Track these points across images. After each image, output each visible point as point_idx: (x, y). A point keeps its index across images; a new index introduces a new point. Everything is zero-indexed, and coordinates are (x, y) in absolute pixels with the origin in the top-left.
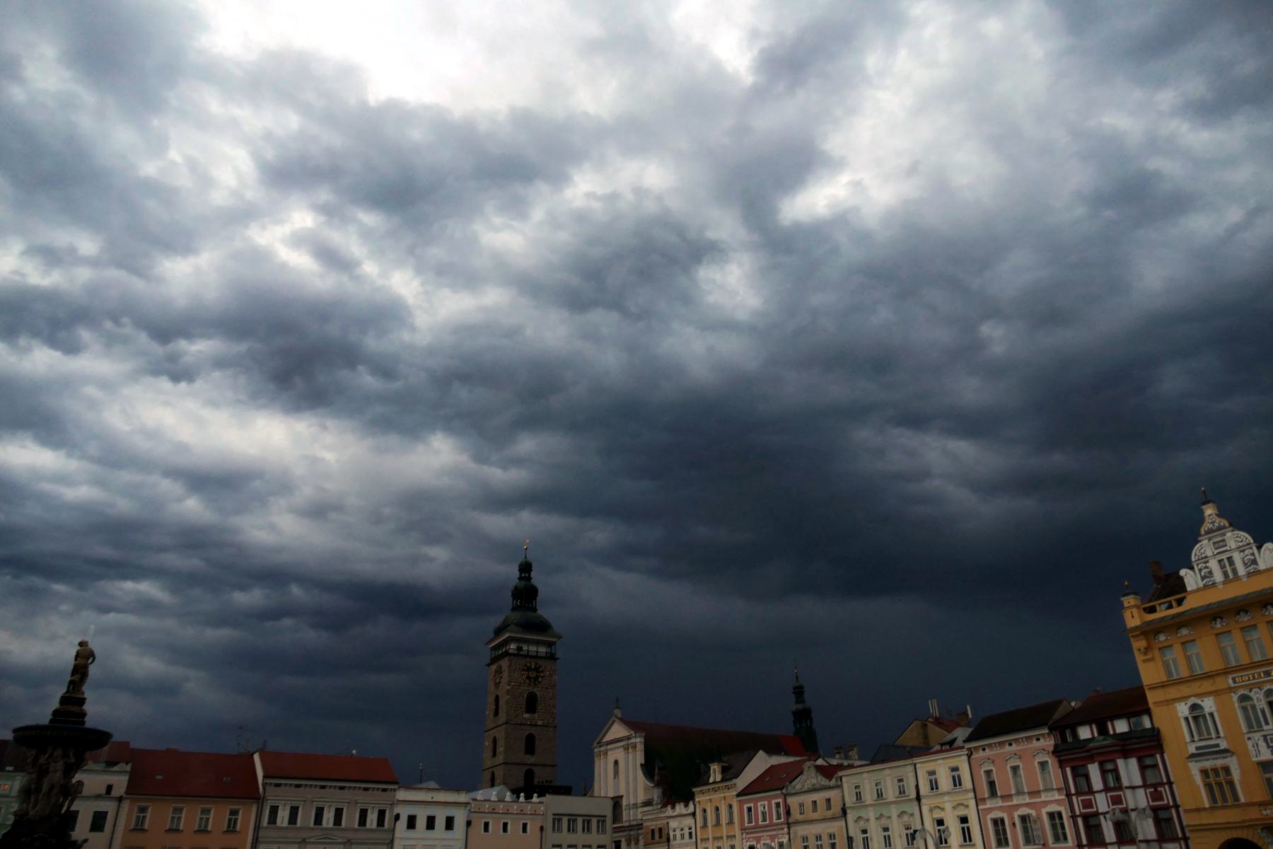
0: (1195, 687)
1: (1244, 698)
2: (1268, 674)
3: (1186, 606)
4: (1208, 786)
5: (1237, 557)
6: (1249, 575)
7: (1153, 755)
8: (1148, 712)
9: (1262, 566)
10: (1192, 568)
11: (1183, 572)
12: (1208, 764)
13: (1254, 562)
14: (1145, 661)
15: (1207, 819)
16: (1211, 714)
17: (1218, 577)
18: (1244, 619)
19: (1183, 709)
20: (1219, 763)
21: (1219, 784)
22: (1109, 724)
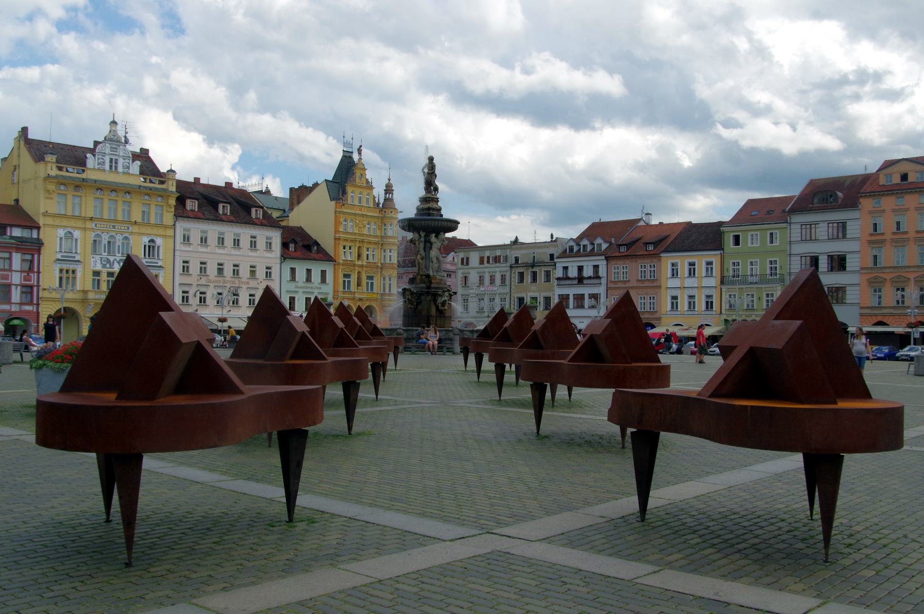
0: (72, 223)
1: (98, 235)
2: (114, 227)
3: (84, 176)
4: (61, 278)
5: (121, 161)
6: (124, 173)
7: (33, 255)
8: (39, 228)
9: (131, 172)
10: (94, 156)
11: (89, 155)
12: (65, 266)
13: (128, 168)
14: (47, 198)
15: (54, 295)
16: (76, 240)
17: (107, 167)
18: (113, 194)
19: (61, 232)
20: (71, 267)
21: (67, 277)
22: (9, 229)
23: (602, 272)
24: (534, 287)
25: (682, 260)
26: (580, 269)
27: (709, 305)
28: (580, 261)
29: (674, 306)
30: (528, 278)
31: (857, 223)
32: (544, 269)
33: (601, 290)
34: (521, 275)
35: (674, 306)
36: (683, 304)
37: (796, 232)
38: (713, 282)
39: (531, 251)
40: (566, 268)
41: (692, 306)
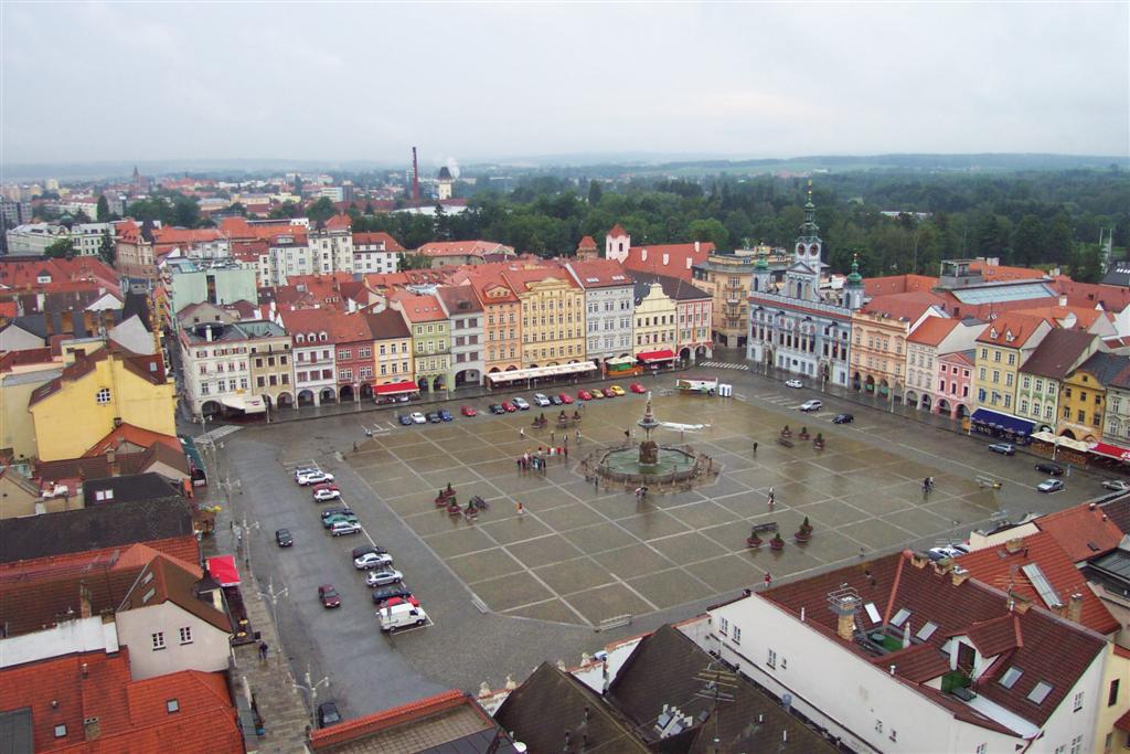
23: (332, 354)
24: (272, 368)
25: (388, 344)
26: (313, 354)
27: (405, 368)
28: (313, 349)
29: (384, 371)
30: (265, 363)
31: (482, 320)
32: (280, 356)
33: (332, 367)
34: (259, 363)
35: (384, 371)
36: (389, 371)
37: (453, 324)
38: (408, 355)
39: (267, 344)
40: (300, 355)
41: (394, 370)
